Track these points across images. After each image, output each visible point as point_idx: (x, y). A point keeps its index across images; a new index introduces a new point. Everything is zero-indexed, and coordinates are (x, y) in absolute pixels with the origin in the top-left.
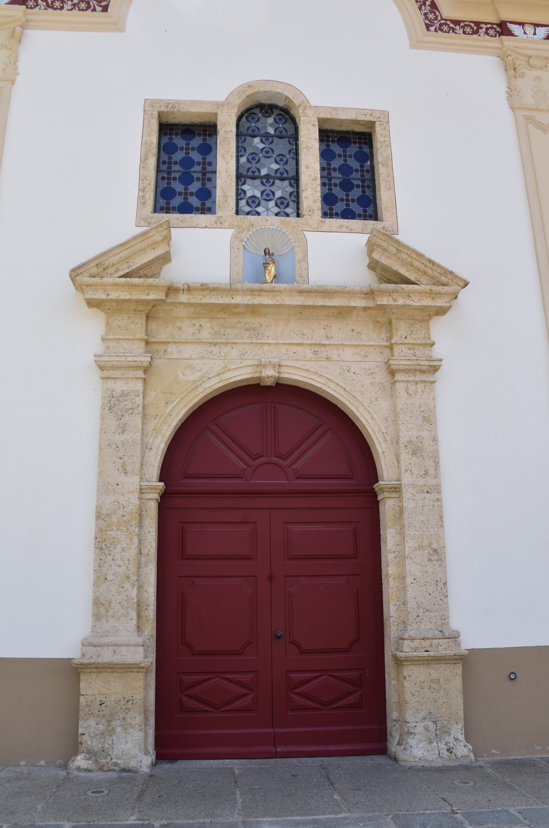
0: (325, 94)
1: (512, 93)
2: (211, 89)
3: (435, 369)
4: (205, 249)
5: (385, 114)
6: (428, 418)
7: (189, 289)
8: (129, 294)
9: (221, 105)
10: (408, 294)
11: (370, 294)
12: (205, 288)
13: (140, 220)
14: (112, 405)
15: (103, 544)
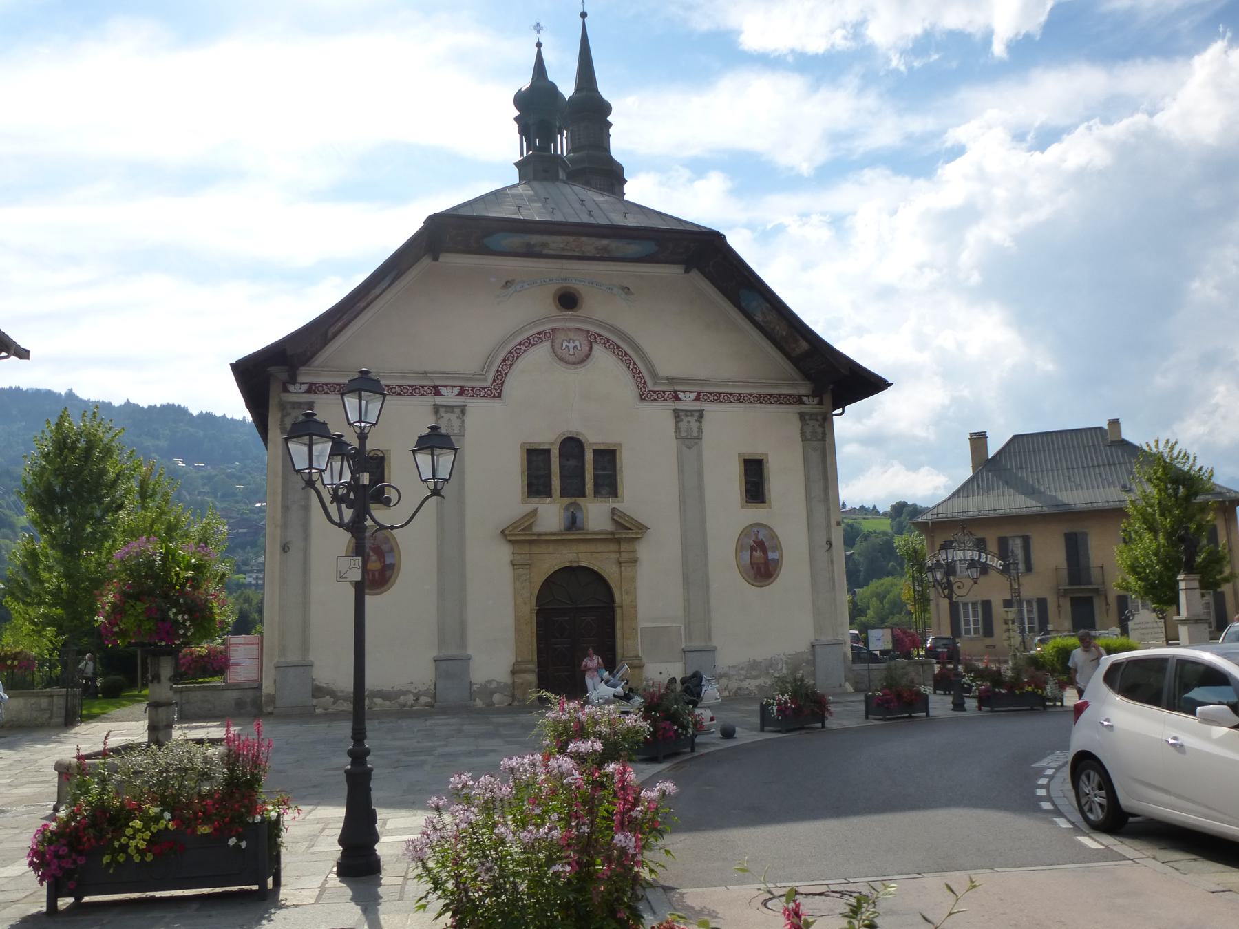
0: (594, 438)
1: (677, 429)
2: (547, 436)
3: (635, 562)
4: (550, 514)
5: (620, 445)
6: (633, 579)
7: (546, 534)
8: (521, 536)
9: (552, 444)
10: (626, 532)
11: (612, 533)
12: (552, 534)
13: (524, 502)
14: (517, 578)
15: (518, 630)
